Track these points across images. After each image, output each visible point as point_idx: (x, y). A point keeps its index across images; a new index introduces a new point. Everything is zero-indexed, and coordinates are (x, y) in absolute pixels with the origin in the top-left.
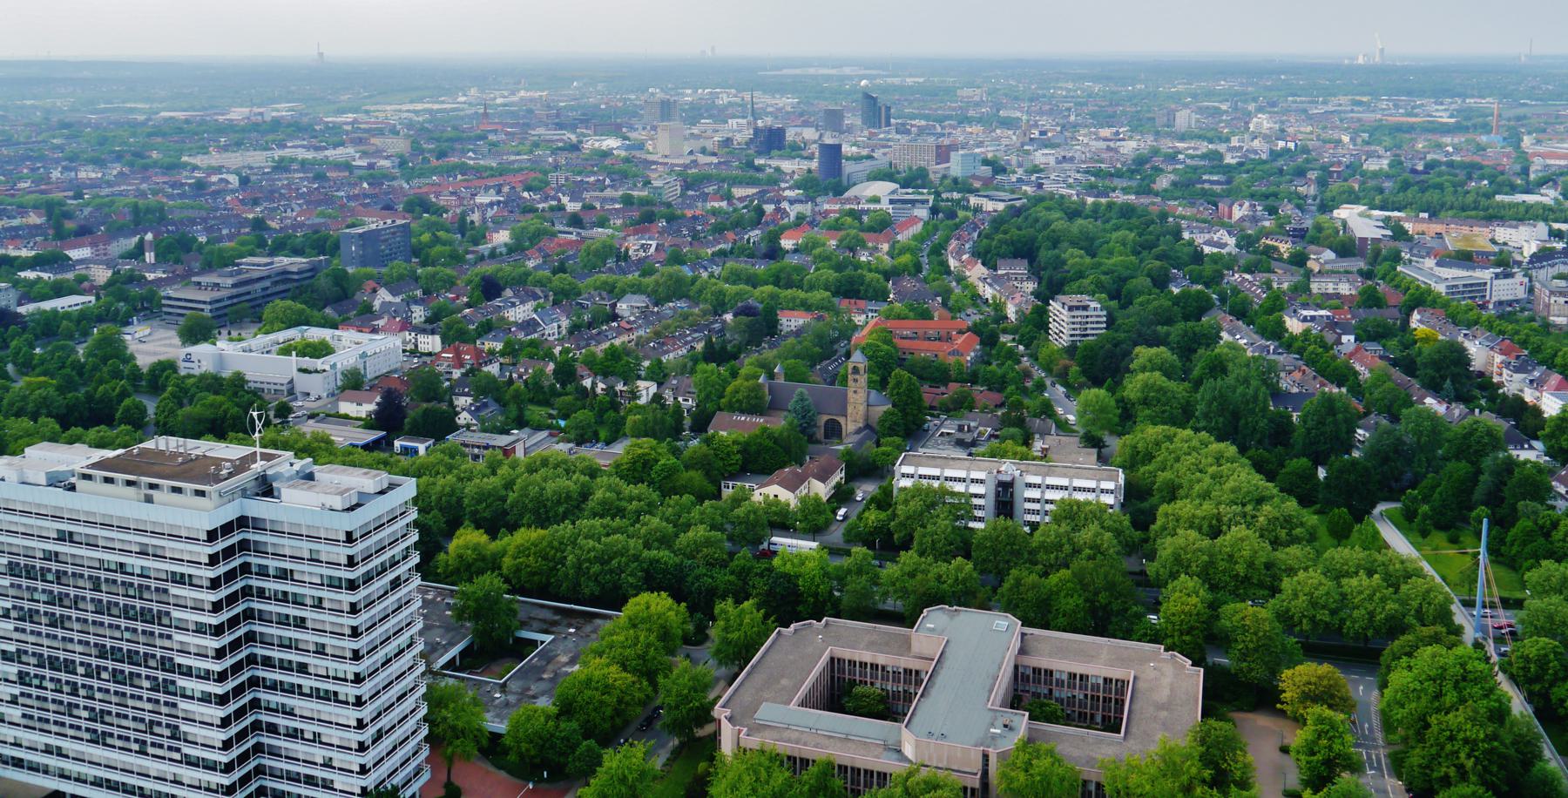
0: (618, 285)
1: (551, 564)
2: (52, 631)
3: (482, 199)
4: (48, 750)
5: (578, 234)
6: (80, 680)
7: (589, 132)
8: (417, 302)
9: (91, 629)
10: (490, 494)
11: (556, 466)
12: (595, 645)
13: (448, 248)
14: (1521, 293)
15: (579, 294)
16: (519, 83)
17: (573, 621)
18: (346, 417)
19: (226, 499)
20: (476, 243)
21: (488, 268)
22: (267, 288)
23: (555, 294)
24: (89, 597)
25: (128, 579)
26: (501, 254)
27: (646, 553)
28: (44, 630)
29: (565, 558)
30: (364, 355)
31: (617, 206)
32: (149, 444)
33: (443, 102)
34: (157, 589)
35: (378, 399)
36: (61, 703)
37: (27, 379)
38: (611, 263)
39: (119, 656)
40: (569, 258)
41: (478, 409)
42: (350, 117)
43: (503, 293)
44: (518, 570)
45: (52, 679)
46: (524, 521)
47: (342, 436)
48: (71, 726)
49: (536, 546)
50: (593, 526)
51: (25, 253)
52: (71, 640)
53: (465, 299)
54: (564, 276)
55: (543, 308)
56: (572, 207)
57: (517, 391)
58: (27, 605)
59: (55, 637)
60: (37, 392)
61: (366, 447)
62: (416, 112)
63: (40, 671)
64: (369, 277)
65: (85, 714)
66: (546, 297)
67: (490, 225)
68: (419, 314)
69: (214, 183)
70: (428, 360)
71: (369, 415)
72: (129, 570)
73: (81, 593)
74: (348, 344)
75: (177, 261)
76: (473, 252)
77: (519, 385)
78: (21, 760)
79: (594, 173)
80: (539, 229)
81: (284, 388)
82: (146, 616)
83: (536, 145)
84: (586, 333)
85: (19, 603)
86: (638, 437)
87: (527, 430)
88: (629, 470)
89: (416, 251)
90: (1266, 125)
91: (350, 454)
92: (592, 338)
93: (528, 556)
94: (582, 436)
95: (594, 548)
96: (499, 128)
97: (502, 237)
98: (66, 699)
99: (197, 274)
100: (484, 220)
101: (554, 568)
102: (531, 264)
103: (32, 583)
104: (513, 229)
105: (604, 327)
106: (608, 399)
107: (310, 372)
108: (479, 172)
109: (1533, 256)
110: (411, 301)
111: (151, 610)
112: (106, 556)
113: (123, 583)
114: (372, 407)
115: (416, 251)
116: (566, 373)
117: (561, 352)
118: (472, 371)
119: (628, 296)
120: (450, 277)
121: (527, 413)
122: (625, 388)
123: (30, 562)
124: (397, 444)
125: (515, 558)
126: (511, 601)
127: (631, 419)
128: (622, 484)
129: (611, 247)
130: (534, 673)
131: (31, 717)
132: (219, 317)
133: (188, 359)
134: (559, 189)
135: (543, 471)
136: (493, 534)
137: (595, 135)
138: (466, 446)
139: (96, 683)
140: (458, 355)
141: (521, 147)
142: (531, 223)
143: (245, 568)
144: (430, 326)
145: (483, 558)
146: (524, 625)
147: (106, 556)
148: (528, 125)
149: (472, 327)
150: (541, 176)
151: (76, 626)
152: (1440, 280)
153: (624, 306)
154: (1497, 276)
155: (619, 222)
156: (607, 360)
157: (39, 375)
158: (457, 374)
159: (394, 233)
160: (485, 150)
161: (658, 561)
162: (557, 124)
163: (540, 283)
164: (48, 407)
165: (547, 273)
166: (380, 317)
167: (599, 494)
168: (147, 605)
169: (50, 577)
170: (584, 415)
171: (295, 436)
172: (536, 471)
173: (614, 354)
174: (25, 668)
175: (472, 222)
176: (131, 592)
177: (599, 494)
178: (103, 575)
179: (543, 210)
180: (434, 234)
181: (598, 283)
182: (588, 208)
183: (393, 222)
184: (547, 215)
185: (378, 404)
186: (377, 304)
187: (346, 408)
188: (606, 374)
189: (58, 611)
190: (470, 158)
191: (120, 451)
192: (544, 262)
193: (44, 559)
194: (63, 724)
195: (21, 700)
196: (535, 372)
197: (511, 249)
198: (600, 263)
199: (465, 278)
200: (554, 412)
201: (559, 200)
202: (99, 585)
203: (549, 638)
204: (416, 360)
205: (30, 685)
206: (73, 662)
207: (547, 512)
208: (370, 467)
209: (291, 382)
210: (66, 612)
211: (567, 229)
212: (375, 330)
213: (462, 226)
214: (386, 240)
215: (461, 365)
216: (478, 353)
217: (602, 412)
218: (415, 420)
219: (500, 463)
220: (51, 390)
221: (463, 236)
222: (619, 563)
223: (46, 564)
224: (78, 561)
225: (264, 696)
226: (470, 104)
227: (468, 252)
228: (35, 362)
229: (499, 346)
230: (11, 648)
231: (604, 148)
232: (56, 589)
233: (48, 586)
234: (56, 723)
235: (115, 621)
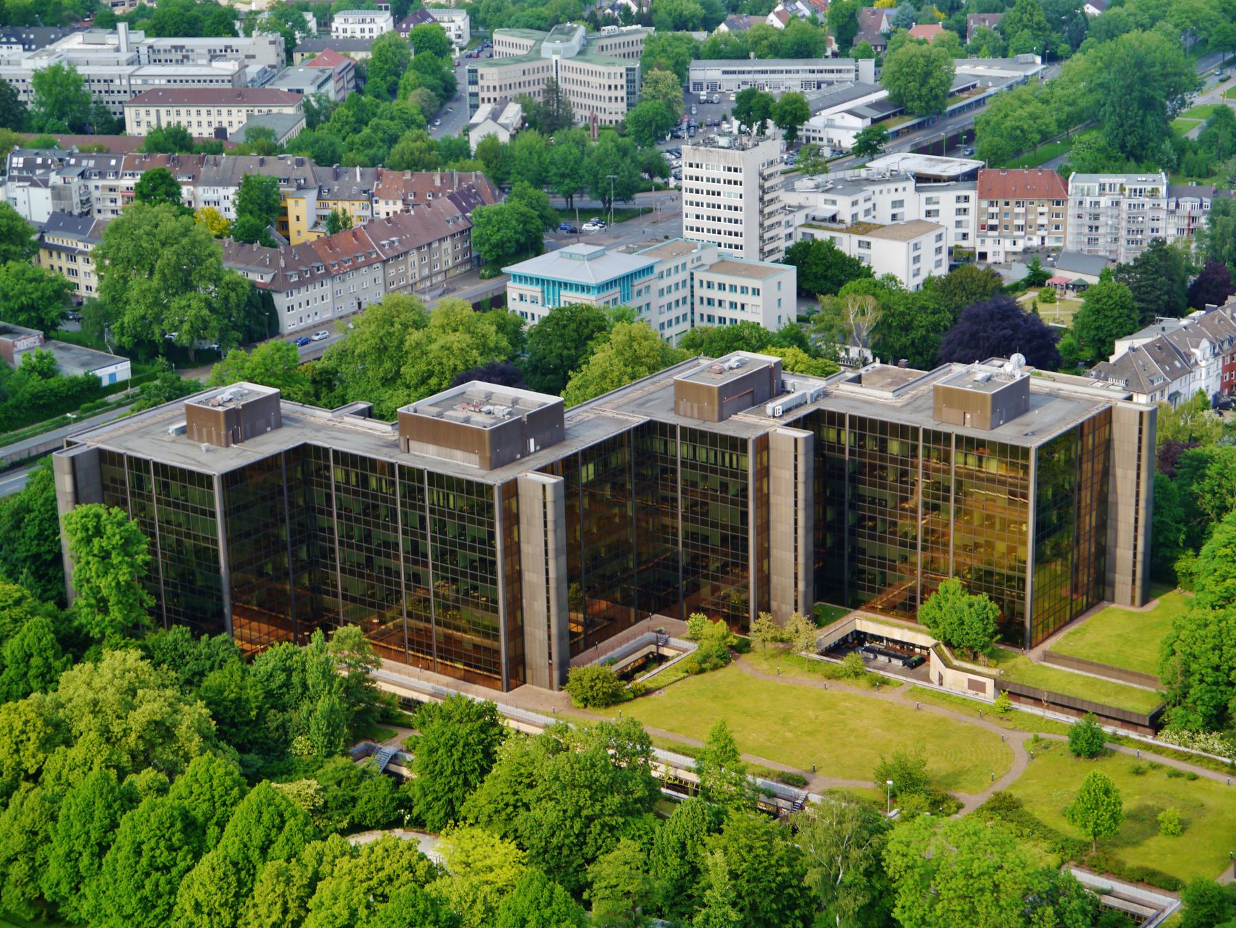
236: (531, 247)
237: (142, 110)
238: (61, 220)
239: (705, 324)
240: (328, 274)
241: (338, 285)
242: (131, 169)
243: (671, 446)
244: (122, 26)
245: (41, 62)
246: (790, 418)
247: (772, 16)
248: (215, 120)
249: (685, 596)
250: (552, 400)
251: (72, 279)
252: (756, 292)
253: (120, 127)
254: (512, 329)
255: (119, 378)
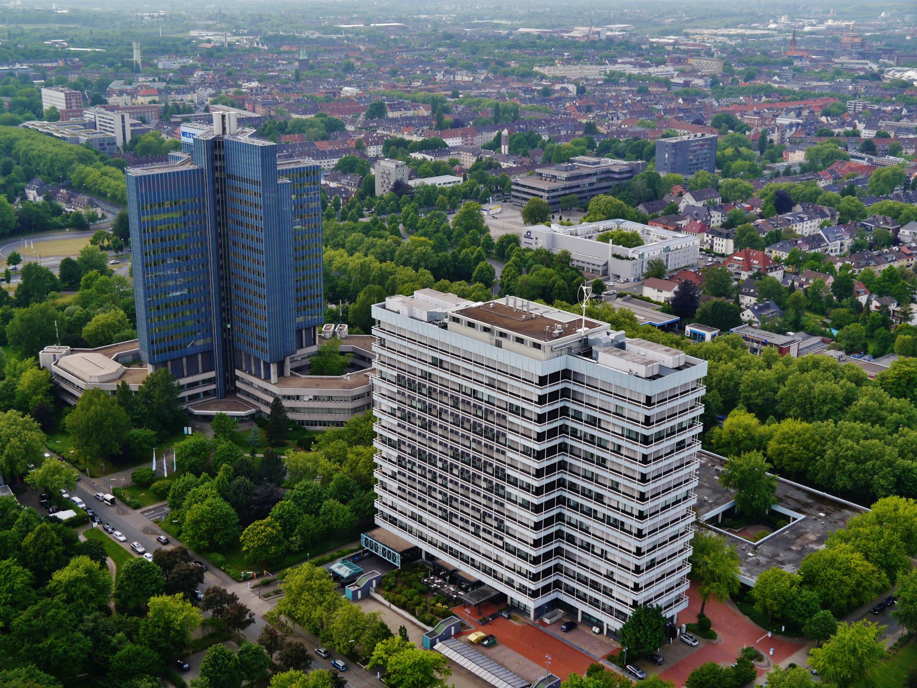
0: (905, 211)
1: (811, 454)
2: (423, 431)
3: (783, 121)
4: (413, 517)
5: (870, 160)
6: (439, 472)
7: (891, 62)
8: (716, 208)
9: (450, 436)
10: (763, 384)
11: (826, 370)
12: (842, 531)
13: (748, 163)
15: (864, 216)
16: (829, 12)
17: (825, 507)
18: (648, 300)
19: (555, 354)
20: (774, 161)
21: (782, 184)
22: (593, 184)
23: (841, 214)
24: (450, 411)
25: (478, 403)
26: (795, 172)
27: (900, 461)
28: (417, 429)
29: (825, 451)
30: (667, 250)
31: (911, 136)
32: (502, 301)
33: (755, 28)
34: (498, 415)
35: (676, 288)
36: (424, 485)
37: (413, 237)
38: (898, 190)
39: (466, 459)
40: (858, 181)
41: (761, 309)
42: (671, 39)
43: (794, 209)
44: (781, 453)
45: (420, 467)
46: (791, 413)
47: (644, 316)
48: (430, 503)
49: (800, 436)
50: (853, 428)
51: (416, 138)
52: (435, 441)
53: (759, 210)
54: (852, 198)
55: (829, 226)
56: (867, 134)
57: (797, 297)
58: (407, 409)
59: (424, 436)
60: (419, 249)
61: (663, 328)
62: (730, 37)
63: (412, 459)
64: (678, 182)
65: (440, 497)
66: (833, 216)
67: (787, 144)
68: (717, 219)
69: (557, 91)
70: (721, 260)
71: (667, 301)
72: (480, 396)
73: (444, 407)
74: (655, 238)
75: (525, 155)
76: (770, 168)
77: (800, 292)
78: (395, 519)
79: (892, 103)
80: (833, 152)
81: (600, 269)
82: (487, 433)
83: (838, 73)
84: (867, 253)
85: (402, 406)
86: (906, 355)
87: (802, 334)
88: (893, 384)
89: (719, 163)
91: (649, 331)
92: (872, 258)
93: (791, 443)
94: (852, 346)
95: (852, 448)
96: (805, 54)
97: (797, 157)
98: (428, 483)
99: (540, 167)
100: (782, 140)
101: (813, 458)
102: (822, 184)
103: (412, 394)
104: (808, 150)
105: (886, 250)
106: (881, 316)
107: (622, 258)
108: (782, 95)
110: (711, 207)
111: (492, 430)
112: (464, 383)
113: (475, 406)
114: (670, 295)
115: (719, 163)
116: (844, 288)
117: (841, 268)
118: (759, 275)
119: (912, 223)
120: (747, 188)
121: (804, 318)
122: (898, 309)
123: (412, 377)
124: (688, 329)
125: (780, 443)
126: (772, 479)
127: (901, 338)
128: (886, 396)
129: (901, 175)
130: (784, 543)
131: (404, 491)
132: (554, 203)
133: (528, 235)
134: (856, 116)
135: (813, 372)
136: (763, 417)
137: (897, 65)
138: (747, 339)
139: (449, 477)
140: (748, 258)
141: (823, 74)
142: (826, 146)
143: (564, 411)
144: (726, 230)
145: (752, 438)
146: (780, 501)
147: (464, 383)
148: (832, 53)
149: (762, 236)
150: (839, 102)
151: (439, 431)
153: (907, 232)
155: (911, 152)
156: (884, 281)
157: (421, 235)
158: (745, 276)
159: (702, 145)
160: (790, 75)
161: (910, 470)
162: (860, 53)
163: (828, 202)
164: (426, 261)
165: (836, 194)
166: (683, 218)
167: (862, 401)
168: (490, 425)
169: (424, 391)
170: (856, 328)
171: (606, 310)
172: (807, 371)
173: (891, 276)
174: (403, 455)
175: (771, 141)
176: (480, 414)
177: (862, 401)
178: (461, 397)
179: (838, 135)
180: (736, 149)
181: (884, 208)
182: (882, 136)
183: (703, 135)
184: (843, 140)
185: (675, 293)
186: (682, 207)
187: (648, 292)
188: (881, 294)
189: (428, 417)
190: (775, 82)
191: (480, 304)
192: (835, 184)
193: (421, 377)
194: (424, 501)
195: (398, 477)
196: (815, 283)
197: (805, 169)
198: (888, 189)
199: (761, 191)
200: (828, 321)
201: (855, 127)
202: (457, 404)
203: (801, 517)
204: (710, 259)
205: (405, 468)
206: (435, 457)
207: (812, 409)
208: (665, 344)
209: (606, 264)
210: (434, 419)
211: (859, 154)
212: (678, 229)
213: (763, 144)
214: (695, 151)
215: (750, 268)
216: (766, 259)
217: (872, 329)
218: (705, 311)
219: (775, 359)
220: (429, 248)
221: (762, 153)
222: (873, 465)
223: (423, 381)
224: (445, 383)
225: (568, 513)
226: (780, 31)
227: (765, 168)
228: (418, 225)
229: (785, 256)
230: (395, 438)
231: (904, 79)
232: (428, 401)
233: (423, 398)
234: (420, 498)
235: (466, 433)
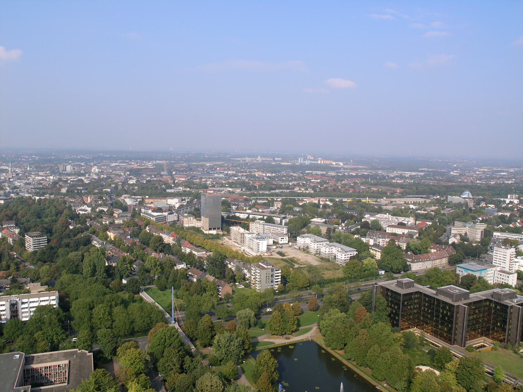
14: (176, 219)
90: (97, 170)
109: (179, 208)
152: (153, 216)
154: (169, 214)
236: (461, 262)
237: (390, 228)
238: (375, 245)
239: (496, 282)
240: (422, 261)
241: (423, 263)
242: (388, 237)
243: (491, 304)
244: (387, 214)
245: (373, 218)
246: (517, 303)
247: (511, 225)
248: (402, 231)
249: (491, 334)
250: (468, 291)
251: (376, 255)
252: (508, 277)
253: (385, 231)
254: (458, 276)
255: (382, 274)
